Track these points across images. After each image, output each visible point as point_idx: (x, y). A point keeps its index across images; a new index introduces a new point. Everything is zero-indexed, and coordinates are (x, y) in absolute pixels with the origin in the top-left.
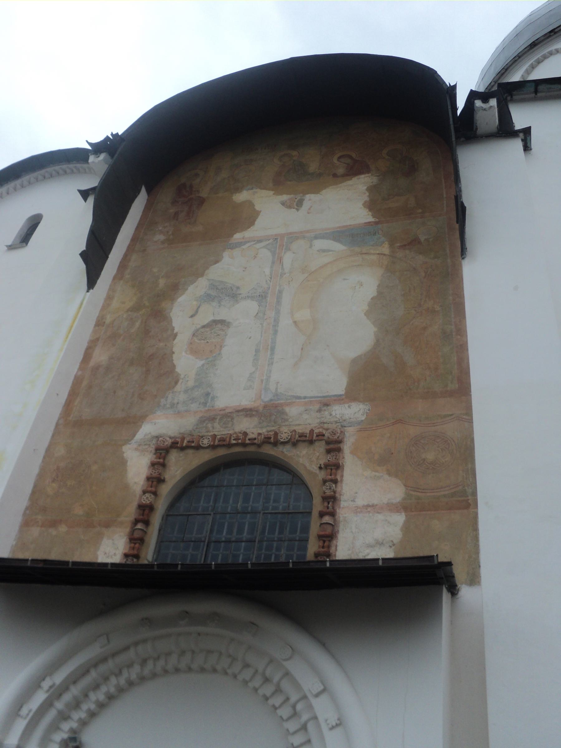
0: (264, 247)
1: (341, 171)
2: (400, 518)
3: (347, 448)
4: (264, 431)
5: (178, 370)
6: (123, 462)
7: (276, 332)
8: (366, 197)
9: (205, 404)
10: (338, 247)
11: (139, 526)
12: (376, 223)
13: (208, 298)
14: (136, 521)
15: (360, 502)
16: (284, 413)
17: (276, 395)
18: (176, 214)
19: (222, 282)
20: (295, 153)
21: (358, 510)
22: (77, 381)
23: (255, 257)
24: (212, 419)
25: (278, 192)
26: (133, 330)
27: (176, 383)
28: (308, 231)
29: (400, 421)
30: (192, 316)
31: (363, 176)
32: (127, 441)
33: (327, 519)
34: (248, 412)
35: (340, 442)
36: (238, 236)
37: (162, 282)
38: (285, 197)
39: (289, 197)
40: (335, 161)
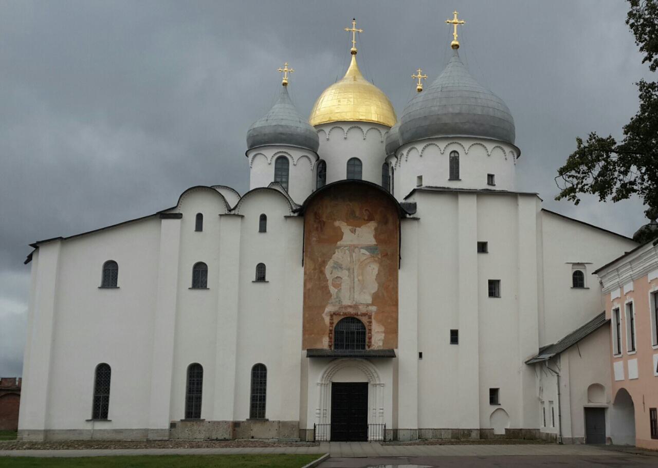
0: (347, 249)
1: (366, 218)
2: (384, 335)
3: (373, 317)
4: (354, 312)
5: (331, 292)
6: (323, 319)
7: (354, 283)
8: (374, 233)
9: (340, 303)
10: (367, 253)
11: (331, 335)
12: (377, 245)
13: (334, 268)
14: (329, 334)
15: (376, 331)
16: (358, 307)
17: (356, 302)
18: (317, 228)
19: (338, 263)
20: (351, 204)
21: (376, 332)
22: (305, 294)
23: (345, 253)
24: (342, 308)
25: (348, 225)
26: (316, 277)
27: (331, 296)
28: (359, 245)
29: (383, 312)
30: (331, 274)
31: (373, 222)
32: (323, 312)
33: (370, 334)
34: (350, 306)
35: (371, 316)
36: (338, 243)
37: (320, 259)
38: (350, 227)
39: (352, 227)
40: (364, 212)
